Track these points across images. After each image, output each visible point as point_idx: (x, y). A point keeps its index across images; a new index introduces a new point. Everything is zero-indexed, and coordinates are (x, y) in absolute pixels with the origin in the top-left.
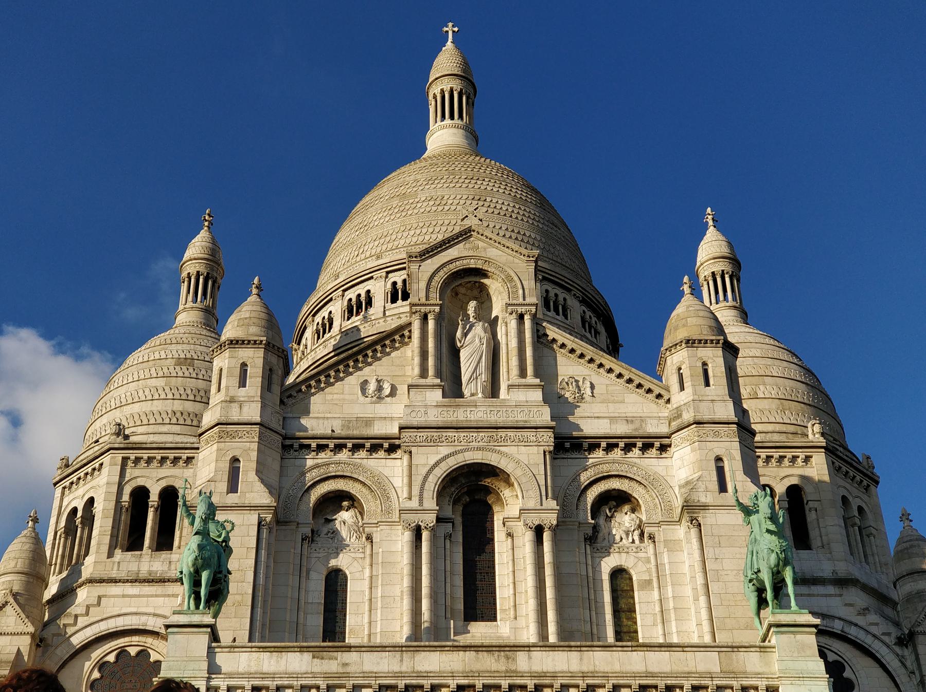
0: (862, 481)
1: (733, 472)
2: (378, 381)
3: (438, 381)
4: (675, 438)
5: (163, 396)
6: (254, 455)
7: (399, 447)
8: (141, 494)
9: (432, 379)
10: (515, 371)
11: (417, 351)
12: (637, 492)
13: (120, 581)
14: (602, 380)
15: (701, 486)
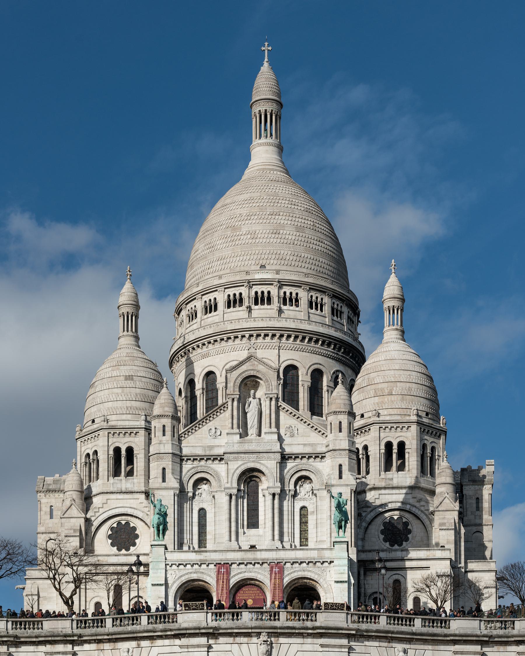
0: (436, 433)
1: (345, 470)
2: (216, 428)
3: (237, 431)
4: (327, 455)
5: (121, 399)
6: (170, 466)
7: (223, 459)
8: (117, 450)
9: (236, 430)
10: (268, 425)
11: (230, 416)
12: (312, 476)
13: (115, 493)
14: (302, 427)
15: (332, 477)
